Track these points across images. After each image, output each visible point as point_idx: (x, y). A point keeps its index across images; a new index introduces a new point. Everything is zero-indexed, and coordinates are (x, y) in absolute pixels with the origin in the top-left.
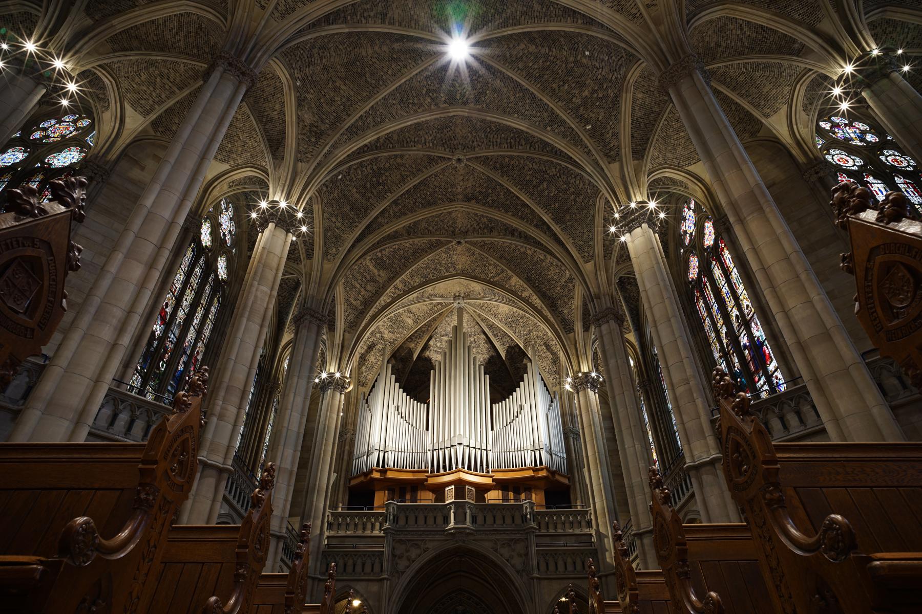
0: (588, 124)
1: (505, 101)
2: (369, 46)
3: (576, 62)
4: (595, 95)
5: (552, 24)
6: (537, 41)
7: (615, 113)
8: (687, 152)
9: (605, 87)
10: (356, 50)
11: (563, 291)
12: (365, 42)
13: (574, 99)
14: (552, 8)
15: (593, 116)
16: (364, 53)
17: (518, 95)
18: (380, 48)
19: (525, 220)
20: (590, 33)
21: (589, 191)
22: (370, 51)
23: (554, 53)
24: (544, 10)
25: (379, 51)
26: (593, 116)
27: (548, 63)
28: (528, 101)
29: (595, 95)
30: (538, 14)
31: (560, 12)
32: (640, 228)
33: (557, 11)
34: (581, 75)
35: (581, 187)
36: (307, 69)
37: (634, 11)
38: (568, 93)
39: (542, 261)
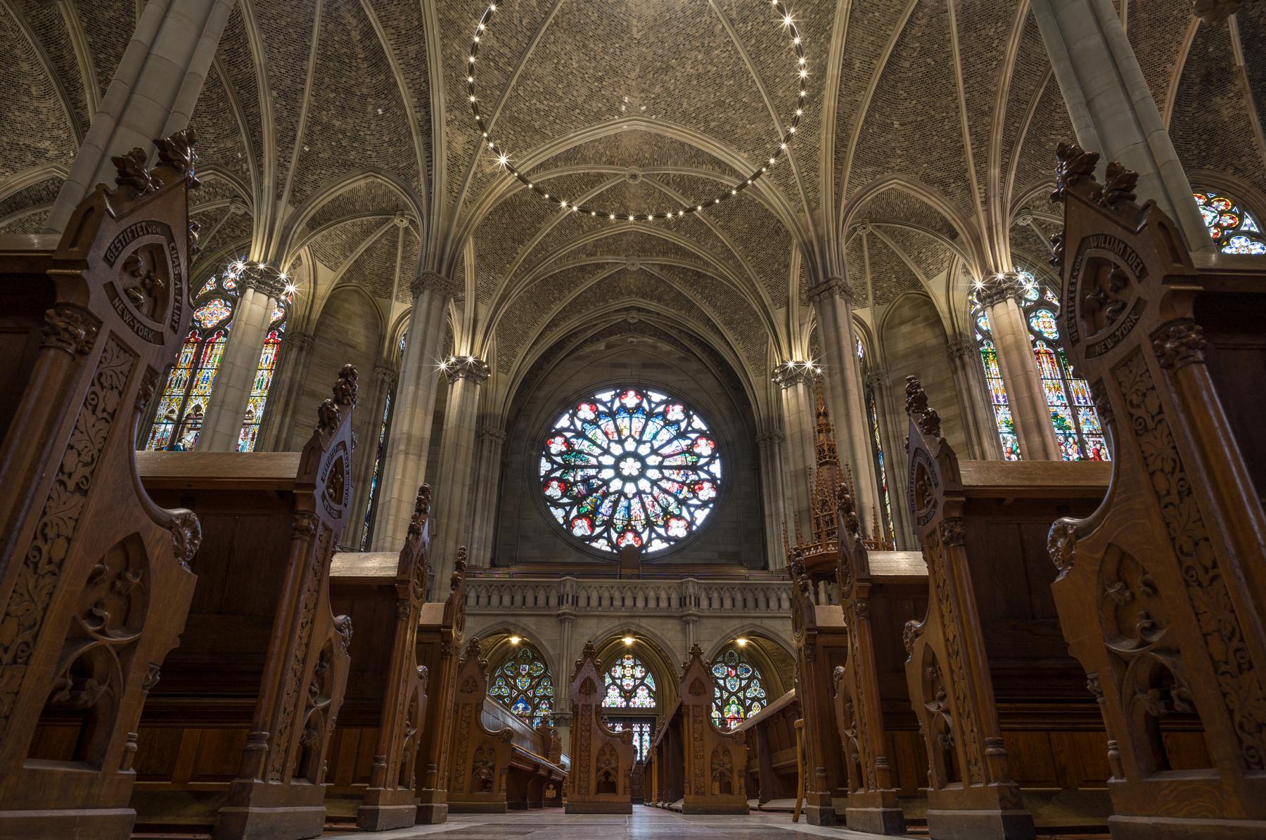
0: (309, 144)
1: (273, 11)
3: (363, 97)
4: (341, 137)
5: (402, 77)
7: (336, 171)
8: (330, 251)
9: (355, 145)
11: (8, 148)
13: (325, 113)
14: (418, 73)
15: (319, 145)
17: (290, 30)
19: (100, 70)
20: (415, 138)
21: (211, 151)
24: (412, 62)
26: (319, 145)
27: (347, 61)
28: (291, 48)
29: (341, 137)
30: (404, 52)
31: (418, 87)
32: (266, 298)
33: (418, 81)
34: (352, 109)
35: (207, 136)
37: (455, 187)
38: (327, 101)
39: (27, 92)
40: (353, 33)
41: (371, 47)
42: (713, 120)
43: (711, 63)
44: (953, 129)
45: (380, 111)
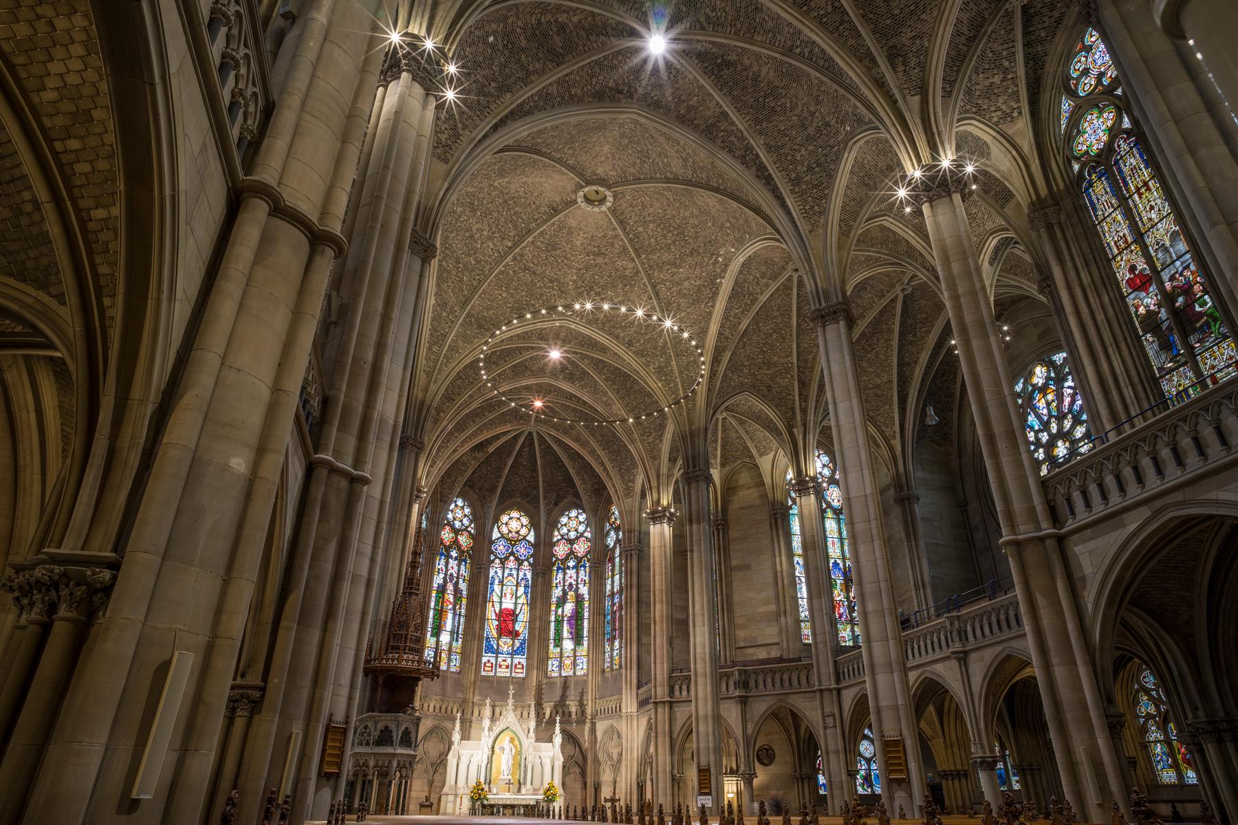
2: (762, 76)
6: (555, 29)
10: (777, 84)
12: (762, 85)
16: (772, 74)
18: (751, 65)
22: (764, 70)
23: (534, 17)
25: (755, 63)
36: (832, 124)
40: (565, 16)
41: (551, 33)
42: (447, 262)
43: (482, 243)
44: (459, 387)
45: (491, 39)
